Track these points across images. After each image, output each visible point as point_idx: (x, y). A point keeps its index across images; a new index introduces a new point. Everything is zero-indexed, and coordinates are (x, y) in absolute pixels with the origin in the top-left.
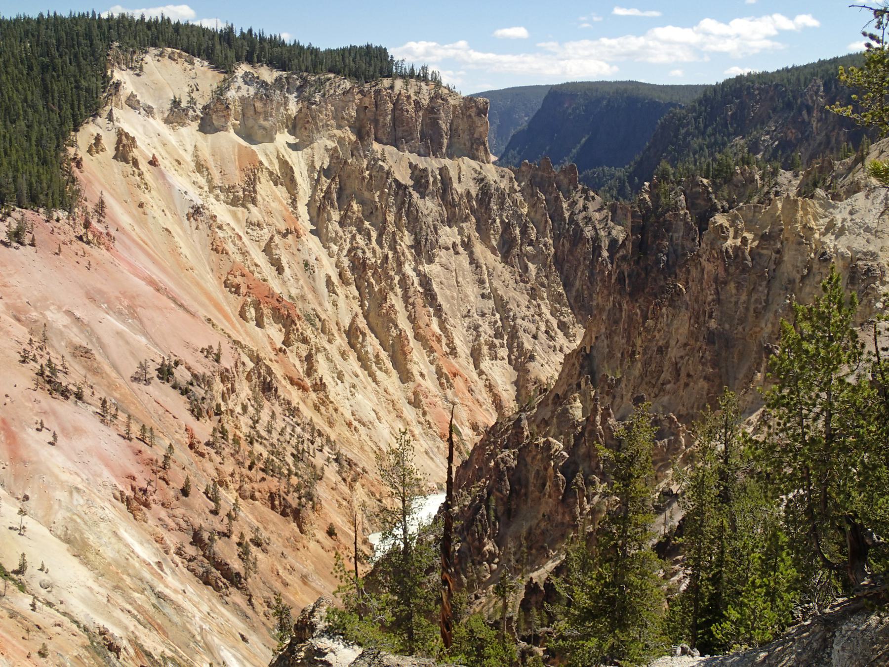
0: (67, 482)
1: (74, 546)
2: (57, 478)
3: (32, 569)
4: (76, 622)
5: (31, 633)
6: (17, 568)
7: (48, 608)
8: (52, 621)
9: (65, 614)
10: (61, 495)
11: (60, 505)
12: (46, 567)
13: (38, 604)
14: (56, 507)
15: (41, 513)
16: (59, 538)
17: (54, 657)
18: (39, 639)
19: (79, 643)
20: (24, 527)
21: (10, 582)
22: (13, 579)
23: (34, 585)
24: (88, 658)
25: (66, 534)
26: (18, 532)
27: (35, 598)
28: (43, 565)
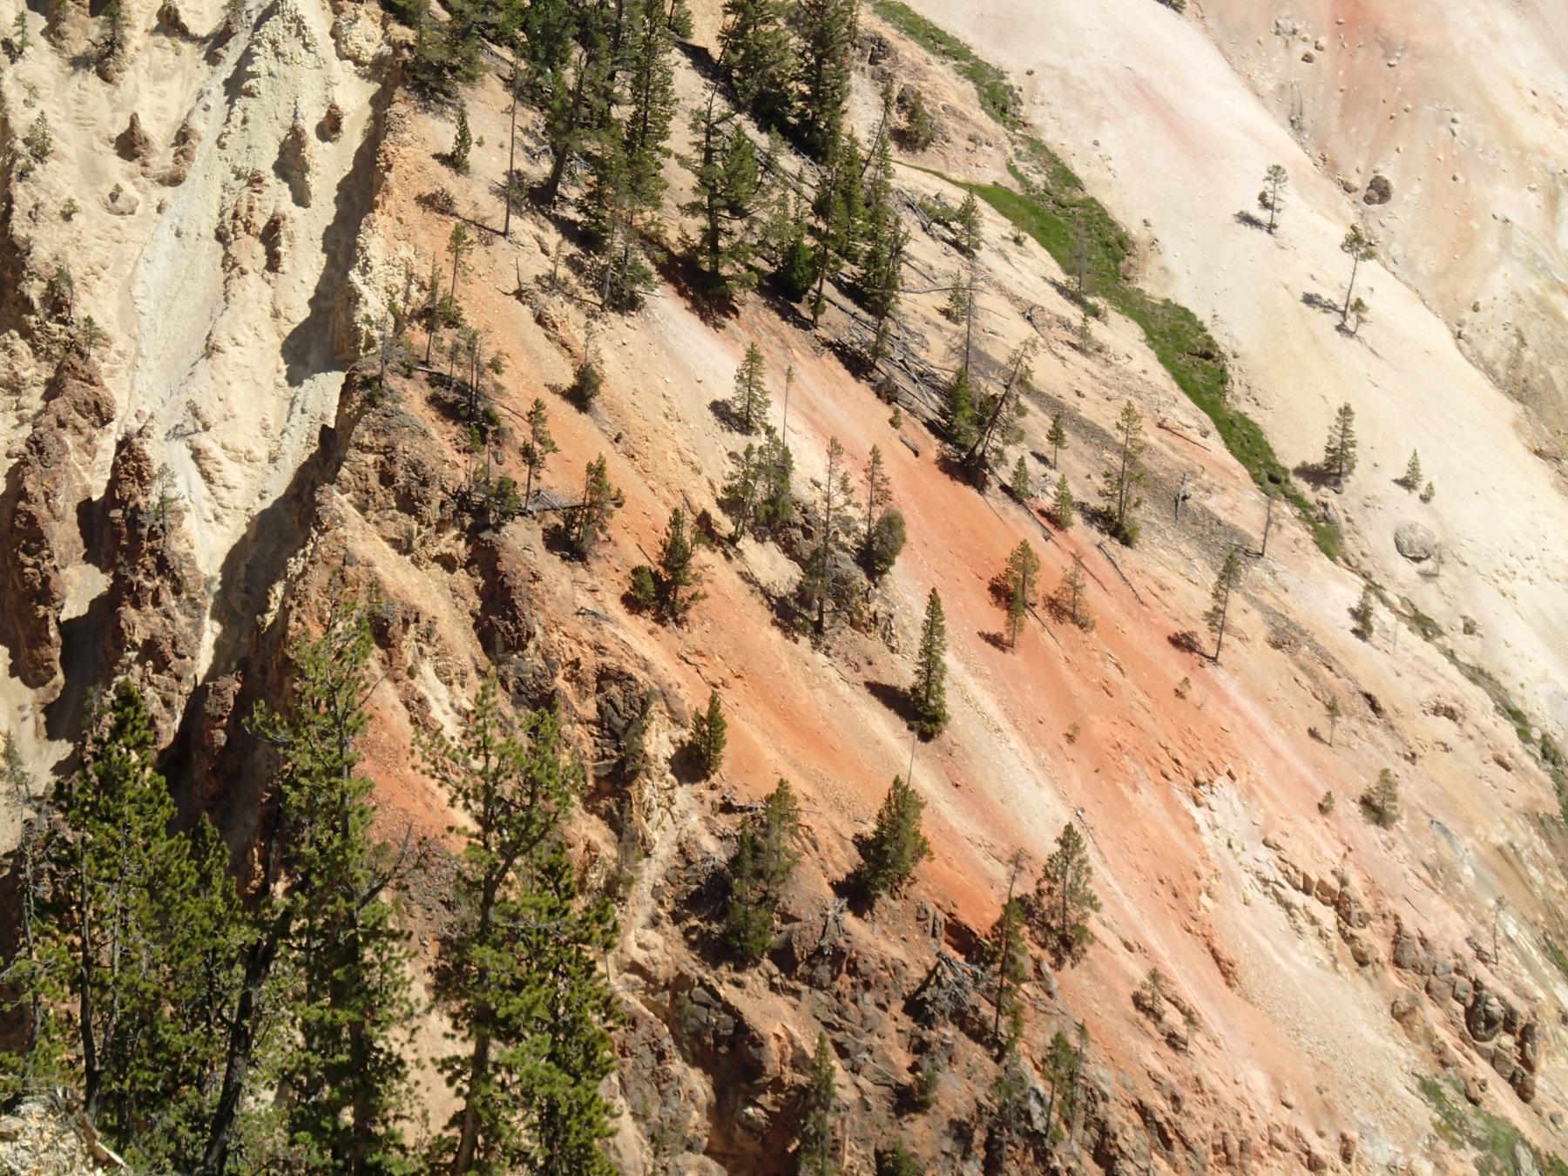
0: (1542, 151)
1: (1540, 416)
2: (1505, 129)
3: (1371, 477)
4: (1515, 715)
5: (1343, 720)
6: (1317, 457)
7: (1416, 639)
8: (1426, 692)
9: (1477, 675)
10: (1512, 200)
11: (1505, 245)
12: (1428, 474)
13: (1381, 615)
14: (1492, 246)
15: (1427, 261)
16: (1490, 371)
17: (1416, 830)
18: (1364, 755)
19: (1518, 802)
20: (1359, 306)
21: (1287, 510)
22: (1296, 500)
23: (1374, 539)
24: (1543, 866)
25: (1515, 364)
26: (1336, 319)
27: (1373, 588)
28: (1414, 466)
